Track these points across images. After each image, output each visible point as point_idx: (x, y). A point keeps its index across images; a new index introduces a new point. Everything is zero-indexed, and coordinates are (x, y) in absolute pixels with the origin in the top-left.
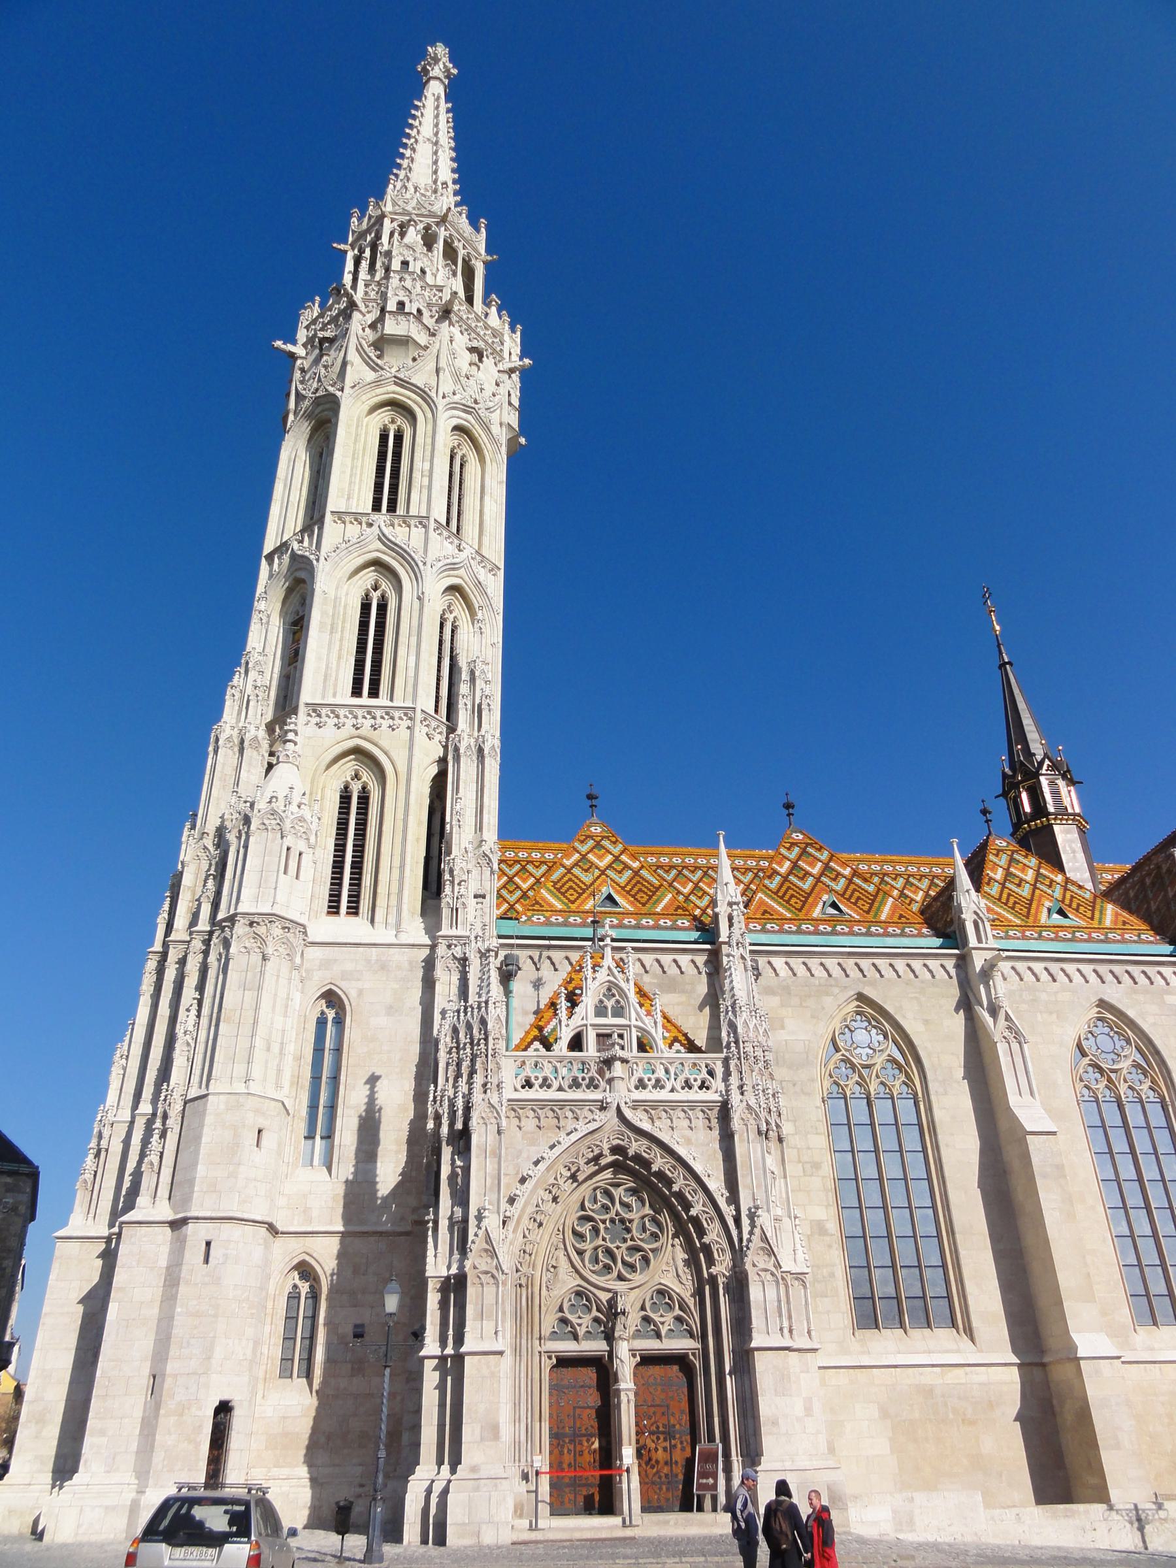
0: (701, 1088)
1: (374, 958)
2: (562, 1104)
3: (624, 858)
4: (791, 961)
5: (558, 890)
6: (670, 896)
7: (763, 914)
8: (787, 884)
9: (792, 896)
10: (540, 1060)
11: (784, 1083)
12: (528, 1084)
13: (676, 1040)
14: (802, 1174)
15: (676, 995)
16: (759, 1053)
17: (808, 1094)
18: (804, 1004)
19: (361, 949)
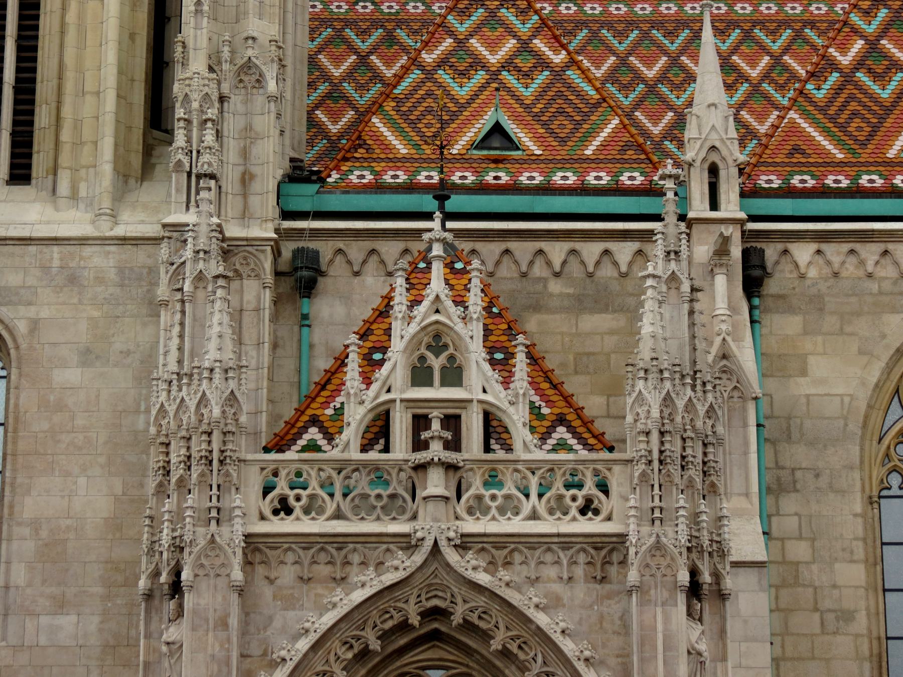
0: (583, 511)
1: (56, 263)
2: (340, 541)
3: (539, 44)
4: (830, 249)
5: (405, 116)
6: (616, 121)
7: (791, 154)
8: (850, 89)
9: (855, 114)
10: (305, 467)
11: (798, 474)
12: (284, 508)
13: (561, 420)
14: (818, 630)
15: (609, 316)
16: (695, 451)
17: (842, 492)
18: (848, 329)
19: (32, 249)
